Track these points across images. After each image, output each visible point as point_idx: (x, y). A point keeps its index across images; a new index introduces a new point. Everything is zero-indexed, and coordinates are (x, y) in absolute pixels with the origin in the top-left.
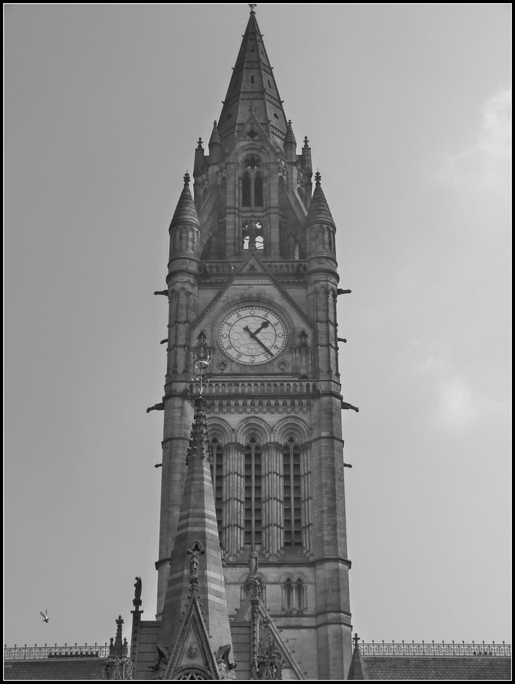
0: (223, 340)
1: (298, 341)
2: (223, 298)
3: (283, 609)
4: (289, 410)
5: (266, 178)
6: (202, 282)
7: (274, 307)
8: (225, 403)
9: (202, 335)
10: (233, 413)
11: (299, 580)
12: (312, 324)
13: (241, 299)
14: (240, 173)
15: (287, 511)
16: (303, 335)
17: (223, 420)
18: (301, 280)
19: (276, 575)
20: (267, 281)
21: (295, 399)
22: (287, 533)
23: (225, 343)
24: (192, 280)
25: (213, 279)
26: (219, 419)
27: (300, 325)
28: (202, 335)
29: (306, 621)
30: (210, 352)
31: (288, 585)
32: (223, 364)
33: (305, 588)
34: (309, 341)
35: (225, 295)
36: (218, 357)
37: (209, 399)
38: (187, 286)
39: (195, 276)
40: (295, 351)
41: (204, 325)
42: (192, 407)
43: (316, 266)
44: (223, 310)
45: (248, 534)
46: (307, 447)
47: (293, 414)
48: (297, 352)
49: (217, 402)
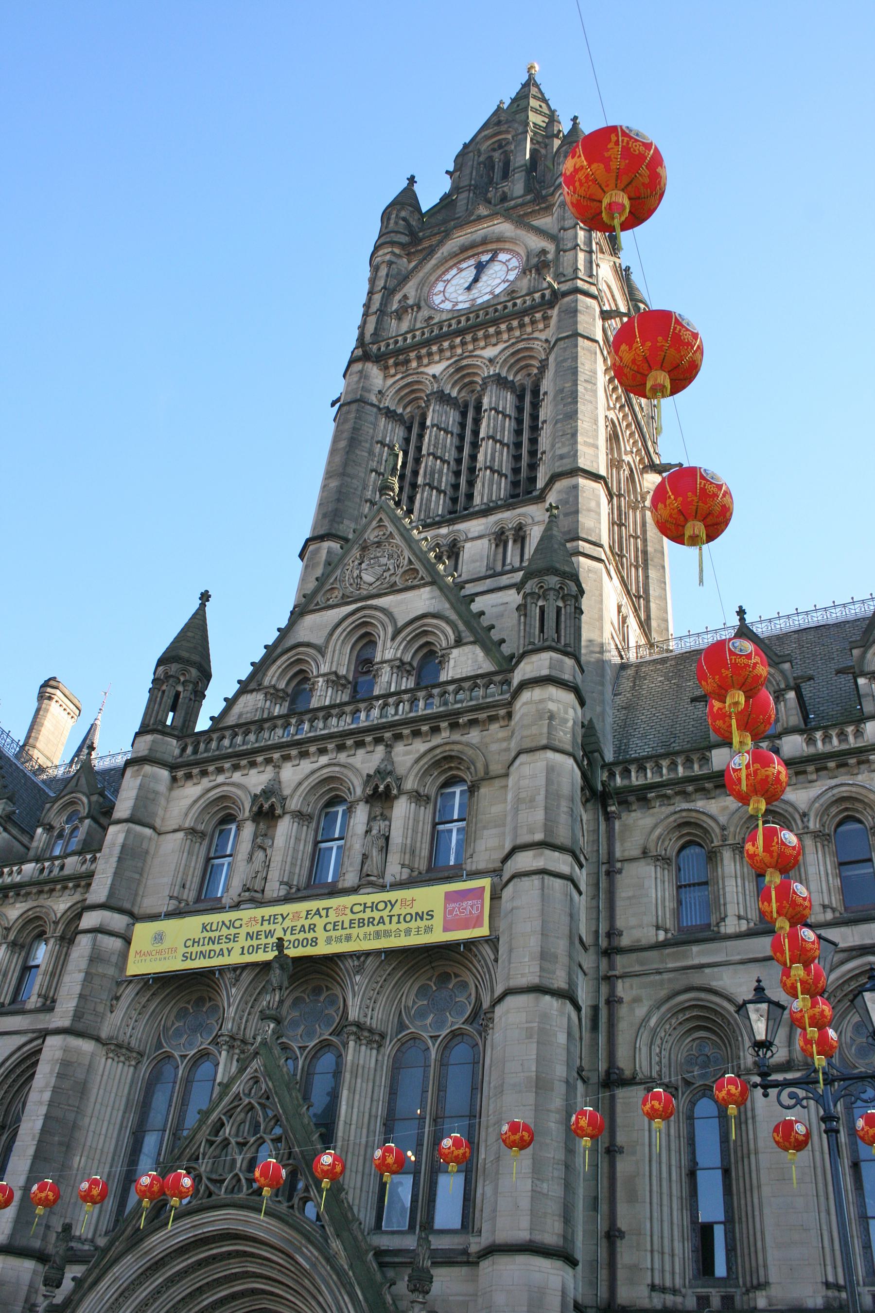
0: (435, 297)
1: (535, 260)
2: (438, 255)
3: (488, 568)
4: (517, 333)
6: (412, 250)
7: (505, 241)
8: (424, 351)
9: (405, 297)
13: (460, 249)
15: (517, 458)
16: (544, 252)
17: (422, 373)
18: (543, 205)
19: (482, 527)
21: (524, 316)
22: (515, 484)
23: (437, 299)
25: (426, 244)
27: (536, 243)
28: (405, 297)
30: (412, 310)
31: (500, 538)
32: (431, 318)
33: (528, 532)
35: (441, 251)
36: (425, 313)
37: (402, 354)
39: (402, 246)
40: (531, 272)
41: (410, 289)
42: (381, 370)
44: (437, 267)
45: (454, 500)
46: (543, 367)
47: (525, 336)
49: (413, 355)
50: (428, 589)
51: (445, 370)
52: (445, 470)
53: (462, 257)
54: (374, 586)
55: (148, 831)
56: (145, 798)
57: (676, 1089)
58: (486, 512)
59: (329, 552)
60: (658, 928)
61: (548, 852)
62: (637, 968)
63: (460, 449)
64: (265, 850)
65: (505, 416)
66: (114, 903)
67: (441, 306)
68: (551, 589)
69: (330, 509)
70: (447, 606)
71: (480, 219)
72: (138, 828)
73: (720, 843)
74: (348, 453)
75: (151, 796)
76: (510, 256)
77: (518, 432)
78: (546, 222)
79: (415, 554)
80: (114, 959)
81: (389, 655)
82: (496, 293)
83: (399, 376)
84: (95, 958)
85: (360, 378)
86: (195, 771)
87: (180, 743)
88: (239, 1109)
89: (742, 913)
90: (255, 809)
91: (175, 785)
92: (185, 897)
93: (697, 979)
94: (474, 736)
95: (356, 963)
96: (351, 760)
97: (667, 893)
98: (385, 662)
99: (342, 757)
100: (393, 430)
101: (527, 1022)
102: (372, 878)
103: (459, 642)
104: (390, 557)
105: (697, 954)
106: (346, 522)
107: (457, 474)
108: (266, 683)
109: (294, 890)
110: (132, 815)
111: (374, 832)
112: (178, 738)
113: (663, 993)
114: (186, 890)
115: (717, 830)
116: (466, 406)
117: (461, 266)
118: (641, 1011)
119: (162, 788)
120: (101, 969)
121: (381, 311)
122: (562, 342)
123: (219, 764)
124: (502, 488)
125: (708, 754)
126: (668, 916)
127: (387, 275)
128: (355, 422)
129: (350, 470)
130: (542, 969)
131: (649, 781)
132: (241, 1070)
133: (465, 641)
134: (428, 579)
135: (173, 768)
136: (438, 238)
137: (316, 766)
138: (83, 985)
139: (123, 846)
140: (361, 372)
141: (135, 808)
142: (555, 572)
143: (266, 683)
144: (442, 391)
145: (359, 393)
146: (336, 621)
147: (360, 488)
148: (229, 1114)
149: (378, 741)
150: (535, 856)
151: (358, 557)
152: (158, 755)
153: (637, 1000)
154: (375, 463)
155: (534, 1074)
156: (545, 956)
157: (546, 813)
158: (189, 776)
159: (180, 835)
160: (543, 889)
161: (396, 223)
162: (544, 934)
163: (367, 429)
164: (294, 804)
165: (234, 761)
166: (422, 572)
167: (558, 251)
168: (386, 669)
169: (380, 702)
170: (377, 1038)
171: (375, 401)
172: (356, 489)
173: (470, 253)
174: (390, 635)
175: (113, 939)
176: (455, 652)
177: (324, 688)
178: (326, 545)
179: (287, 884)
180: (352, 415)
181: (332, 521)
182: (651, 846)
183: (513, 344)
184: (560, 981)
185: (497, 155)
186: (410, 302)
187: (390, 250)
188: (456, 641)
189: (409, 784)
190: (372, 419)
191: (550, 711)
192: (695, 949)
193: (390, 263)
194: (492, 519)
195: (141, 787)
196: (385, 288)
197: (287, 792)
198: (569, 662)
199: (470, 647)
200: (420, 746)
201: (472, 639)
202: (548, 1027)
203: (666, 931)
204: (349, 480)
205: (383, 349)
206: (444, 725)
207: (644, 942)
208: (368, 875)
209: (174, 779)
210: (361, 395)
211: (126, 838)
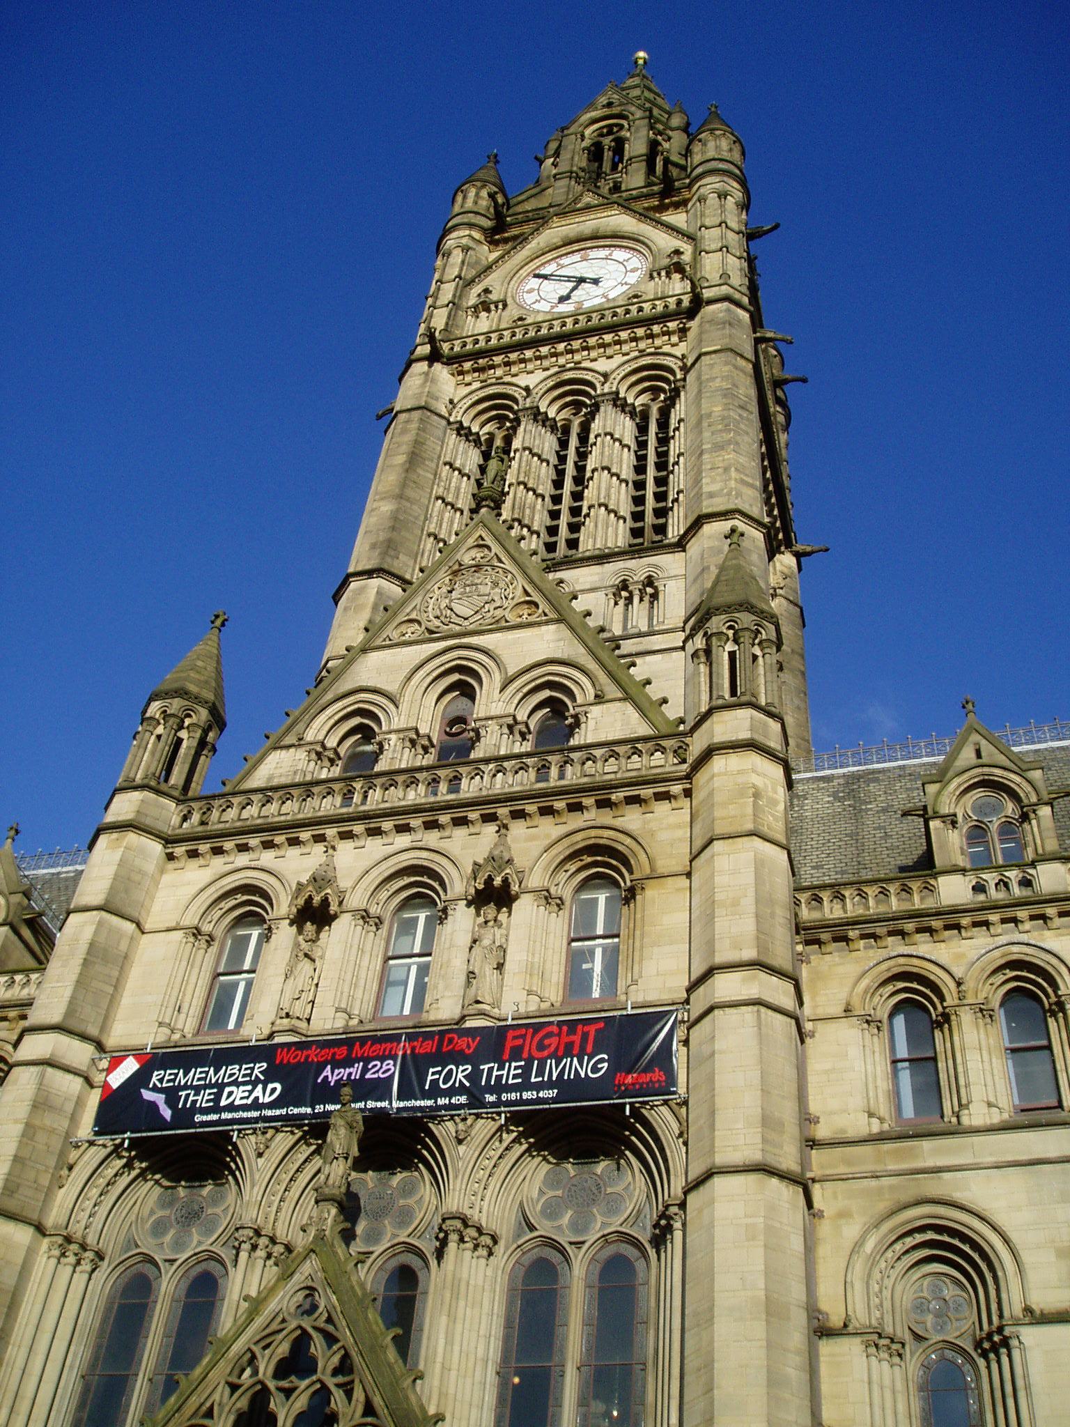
5: (628, 139)
10: (532, 372)
11: (650, 582)
12: (690, 238)
14: (587, 143)
15: (639, 501)
16: (677, 252)
19: (596, 578)
20: (613, 212)
21: (653, 324)
22: (637, 533)
24: (477, 235)
25: (515, 231)
26: (504, 383)
28: (487, 291)
29: (657, 642)
30: (497, 307)
34: (687, 258)
37: (483, 358)
38: (464, 241)
41: (493, 280)
43: (699, 170)
48: (663, 273)
49: (498, 360)
50: (552, 627)
51: (542, 382)
52: (539, 507)
53: (564, 250)
54: (472, 620)
55: (130, 927)
56: (125, 879)
57: (903, 1345)
58: (601, 558)
59: (379, 593)
60: (871, 1115)
61: (763, 976)
62: (842, 1169)
63: (558, 484)
64: (314, 961)
65: (623, 446)
66: (73, 1024)
67: (536, 306)
68: (747, 629)
69: (381, 539)
70: (582, 650)
71: (588, 208)
72: (115, 920)
73: (957, 1002)
74: (407, 471)
75: (137, 878)
76: (630, 256)
77: (640, 469)
78: (677, 218)
79: (532, 582)
80: (69, 1107)
81: (497, 708)
82: (611, 297)
83: (476, 385)
84: (41, 1103)
85: (426, 381)
86: (204, 847)
87: (181, 807)
88: (281, 1336)
89: (992, 1099)
90: (301, 901)
91: (171, 865)
92: (180, 1026)
93: (933, 1186)
94: (632, 819)
95: (461, 1126)
96: (444, 845)
97: (878, 1068)
98: (491, 718)
99: (432, 838)
100: (465, 452)
101: (746, 1216)
102: (487, 1007)
103: (600, 699)
104: (495, 584)
105: (930, 1152)
106: (401, 556)
107: (555, 515)
108: (310, 736)
109: (355, 1022)
110: (107, 900)
111: (486, 942)
112: (179, 801)
113: (883, 1206)
114: (183, 1016)
115: (952, 985)
116: (566, 430)
117: (561, 262)
118: (851, 1231)
119: (151, 867)
120: (48, 1120)
121: (454, 304)
122: (708, 357)
123: (241, 840)
124: (619, 535)
125: (932, 882)
126: (881, 1099)
127: (463, 262)
128: (417, 434)
129: (409, 492)
130: (764, 1140)
131: (849, 914)
132: (286, 1276)
133: (608, 697)
134: (552, 615)
135: (169, 841)
136: (532, 225)
137: (391, 849)
138: (20, 1142)
139: (92, 945)
140: (427, 374)
141: (112, 890)
142: (749, 608)
143: (310, 736)
144: (538, 407)
145: (424, 399)
146: (417, 661)
147: (422, 518)
148: (263, 1344)
149: (488, 818)
150: (744, 980)
151: (447, 581)
152: (148, 821)
153: (843, 1214)
154: (441, 490)
155: (763, 1293)
156: (767, 1121)
157: (758, 922)
158: (193, 854)
159: (180, 934)
160: (759, 1026)
161: (476, 203)
162: (765, 1091)
163: (432, 444)
164: (356, 900)
165: (266, 837)
166: (543, 606)
167: (698, 252)
168: (493, 726)
169: (491, 766)
170: (489, 1241)
171: (444, 412)
172: (416, 518)
173: (575, 247)
174: (498, 685)
175: (70, 1077)
176: (595, 711)
177: (399, 748)
178: (376, 583)
179: (345, 1011)
180: (414, 425)
181: (384, 554)
182: (856, 1002)
183: (636, 358)
184: (788, 1160)
185: (607, 141)
186: (494, 297)
187: (467, 232)
188: (597, 696)
189: (536, 880)
190: (440, 433)
191: (754, 786)
192: (926, 1145)
193: (466, 249)
194: (610, 568)
195: (122, 863)
196: (459, 277)
197: (344, 882)
198: (775, 726)
199: (618, 704)
200: (549, 829)
201: (620, 695)
202: (778, 1225)
203: (881, 1120)
204: (408, 505)
205: (457, 349)
206: (588, 801)
207: (851, 1134)
208: (478, 1002)
209: (171, 857)
210: (426, 402)
211: (96, 933)
